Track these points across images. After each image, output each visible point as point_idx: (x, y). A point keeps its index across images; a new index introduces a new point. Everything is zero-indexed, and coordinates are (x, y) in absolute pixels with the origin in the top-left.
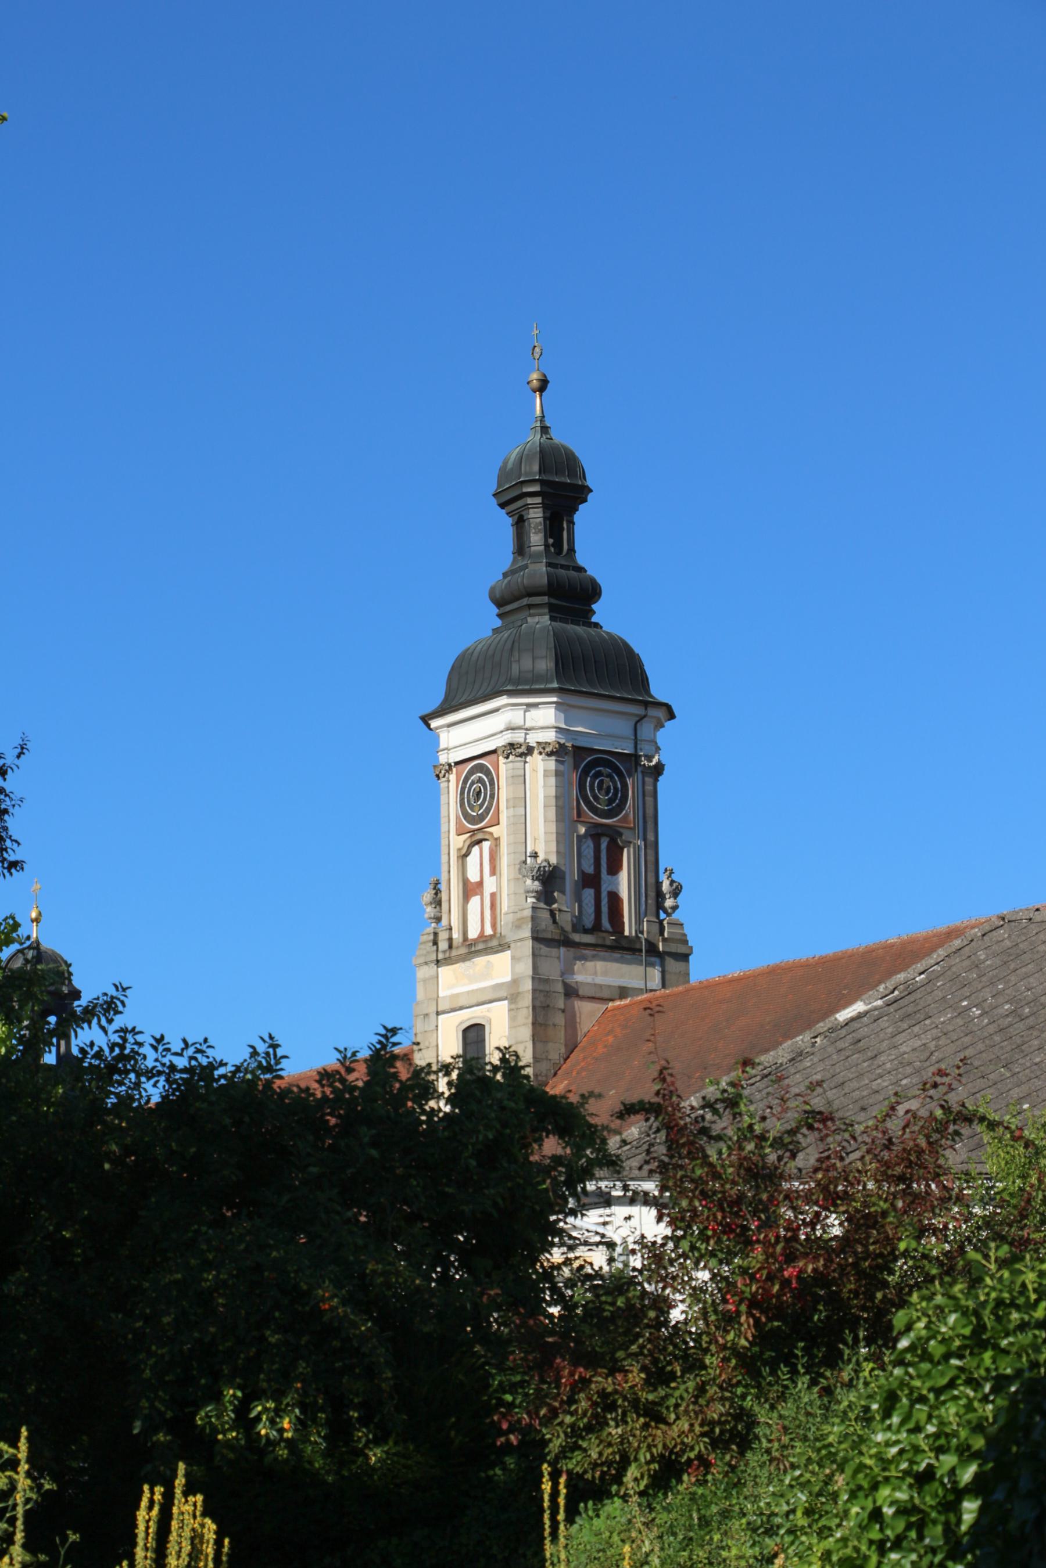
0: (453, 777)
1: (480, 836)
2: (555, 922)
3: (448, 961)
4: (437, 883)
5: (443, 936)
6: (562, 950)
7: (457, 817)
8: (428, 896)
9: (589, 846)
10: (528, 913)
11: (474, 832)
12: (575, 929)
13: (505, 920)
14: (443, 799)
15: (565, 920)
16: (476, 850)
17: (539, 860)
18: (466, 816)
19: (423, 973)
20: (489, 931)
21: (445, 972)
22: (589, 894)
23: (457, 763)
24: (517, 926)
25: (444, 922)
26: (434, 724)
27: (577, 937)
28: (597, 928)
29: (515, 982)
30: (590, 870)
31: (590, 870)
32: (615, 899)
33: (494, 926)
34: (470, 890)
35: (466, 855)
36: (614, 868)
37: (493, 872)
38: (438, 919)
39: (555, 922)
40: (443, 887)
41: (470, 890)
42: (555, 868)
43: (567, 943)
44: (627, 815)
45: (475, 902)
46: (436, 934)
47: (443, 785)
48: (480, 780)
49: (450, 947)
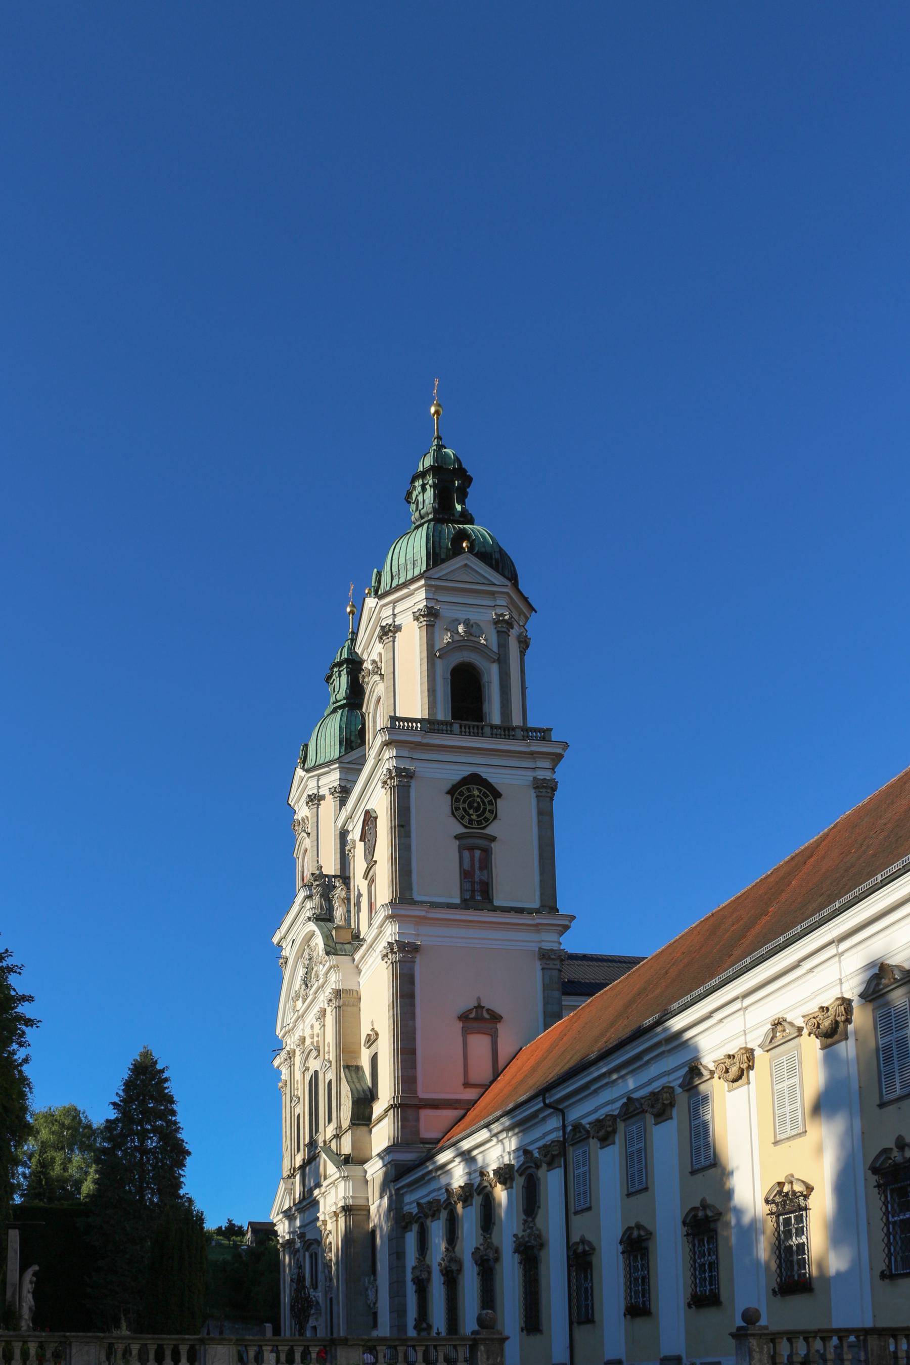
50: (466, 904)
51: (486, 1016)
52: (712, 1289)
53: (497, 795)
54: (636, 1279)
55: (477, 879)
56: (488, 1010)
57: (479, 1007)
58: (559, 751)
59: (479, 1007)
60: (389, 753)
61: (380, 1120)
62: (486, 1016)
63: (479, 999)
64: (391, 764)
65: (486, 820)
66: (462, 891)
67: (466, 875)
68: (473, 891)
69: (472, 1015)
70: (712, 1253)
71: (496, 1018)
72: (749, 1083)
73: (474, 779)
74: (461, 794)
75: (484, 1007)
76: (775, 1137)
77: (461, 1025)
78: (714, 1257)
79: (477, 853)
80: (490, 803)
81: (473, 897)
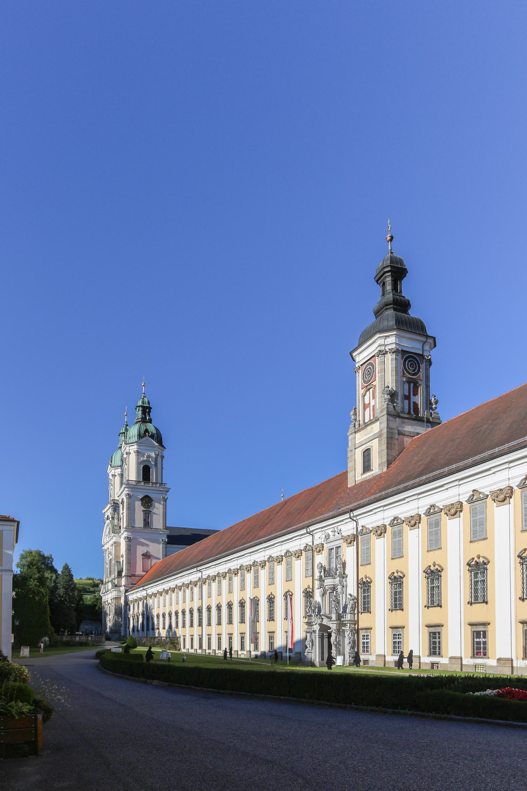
0: (360, 371)
1: (369, 387)
2: (395, 409)
3: (359, 431)
4: (356, 408)
5: (357, 423)
6: (397, 419)
7: (362, 383)
8: (352, 413)
9: (406, 386)
10: (386, 406)
11: (367, 386)
12: (402, 412)
13: (378, 411)
14: (357, 379)
15: (399, 409)
16: (368, 393)
17: (390, 389)
18: (365, 382)
19: (350, 437)
20: (372, 418)
21: (358, 435)
22: (406, 402)
23: (361, 365)
24: (382, 412)
25: (358, 419)
26: (354, 354)
27: (401, 415)
28: (409, 413)
29: (381, 431)
30: (407, 394)
31: (407, 394)
32: (415, 405)
33: (374, 416)
34: (365, 407)
35: (365, 396)
36: (416, 393)
37: (373, 398)
38: (355, 420)
39: (395, 409)
40: (357, 408)
41: (365, 407)
42: (395, 391)
43: (399, 417)
44: (420, 376)
45: (367, 410)
46: (355, 424)
47: (357, 374)
48: (370, 368)
49: (359, 426)
53: (152, 500)
55: (147, 521)
58: (168, 490)
60: (126, 489)
64: (127, 492)
65: (150, 506)
67: (145, 520)
68: (146, 524)
73: (147, 496)
74: (144, 500)
79: (147, 515)
80: (151, 502)
81: (146, 526)
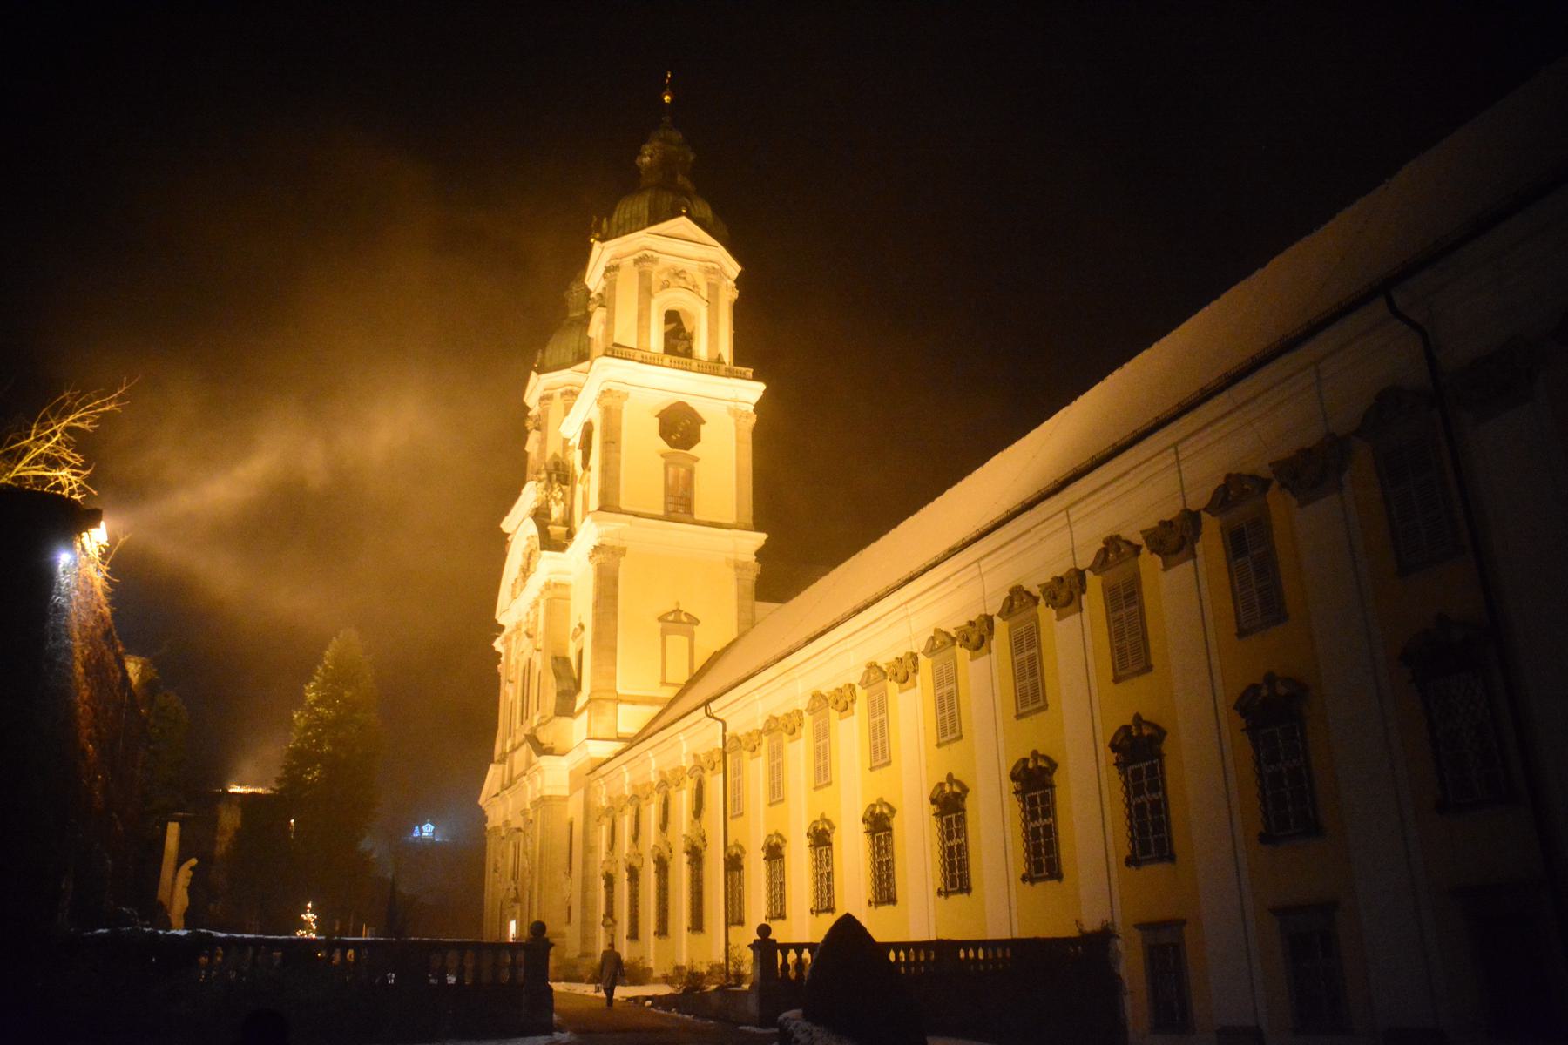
50: (667, 517)
51: (684, 619)
52: (962, 875)
54: (822, 875)
56: (686, 614)
57: (677, 611)
59: (677, 611)
61: (582, 710)
62: (684, 619)
63: (678, 604)
66: (666, 503)
69: (671, 618)
70: (960, 835)
71: (694, 621)
72: (990, 652)
75: (681, 611)
76: (1017, 710)
77: (659, 625)
78: (963, 840)
